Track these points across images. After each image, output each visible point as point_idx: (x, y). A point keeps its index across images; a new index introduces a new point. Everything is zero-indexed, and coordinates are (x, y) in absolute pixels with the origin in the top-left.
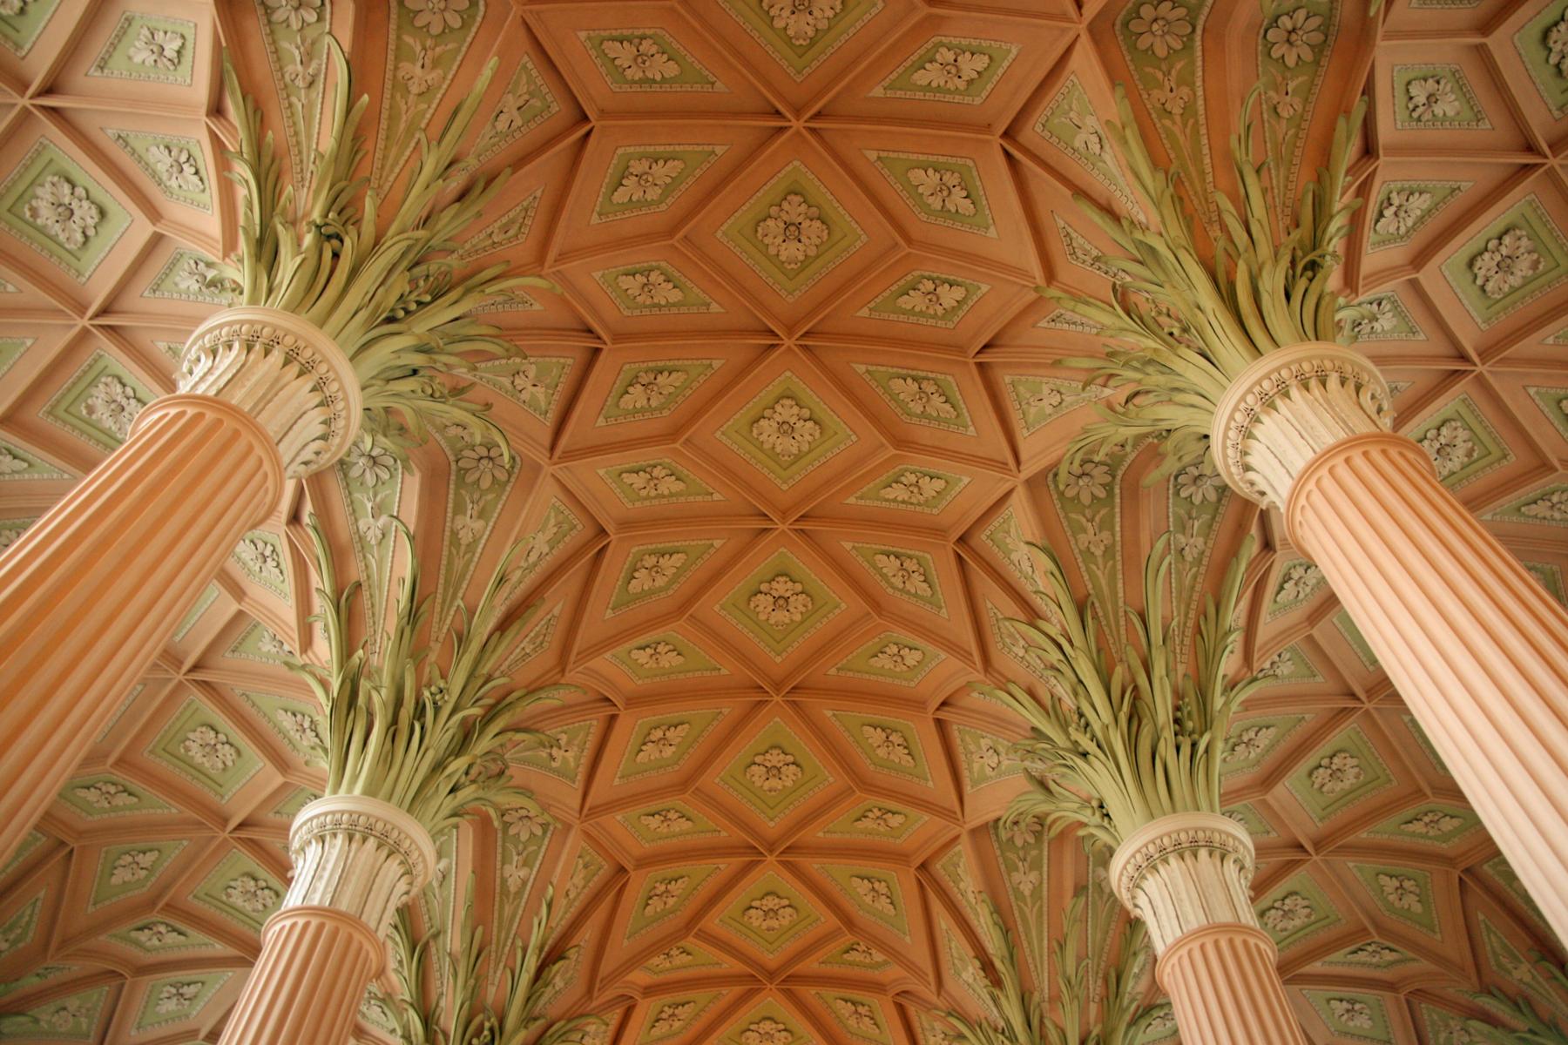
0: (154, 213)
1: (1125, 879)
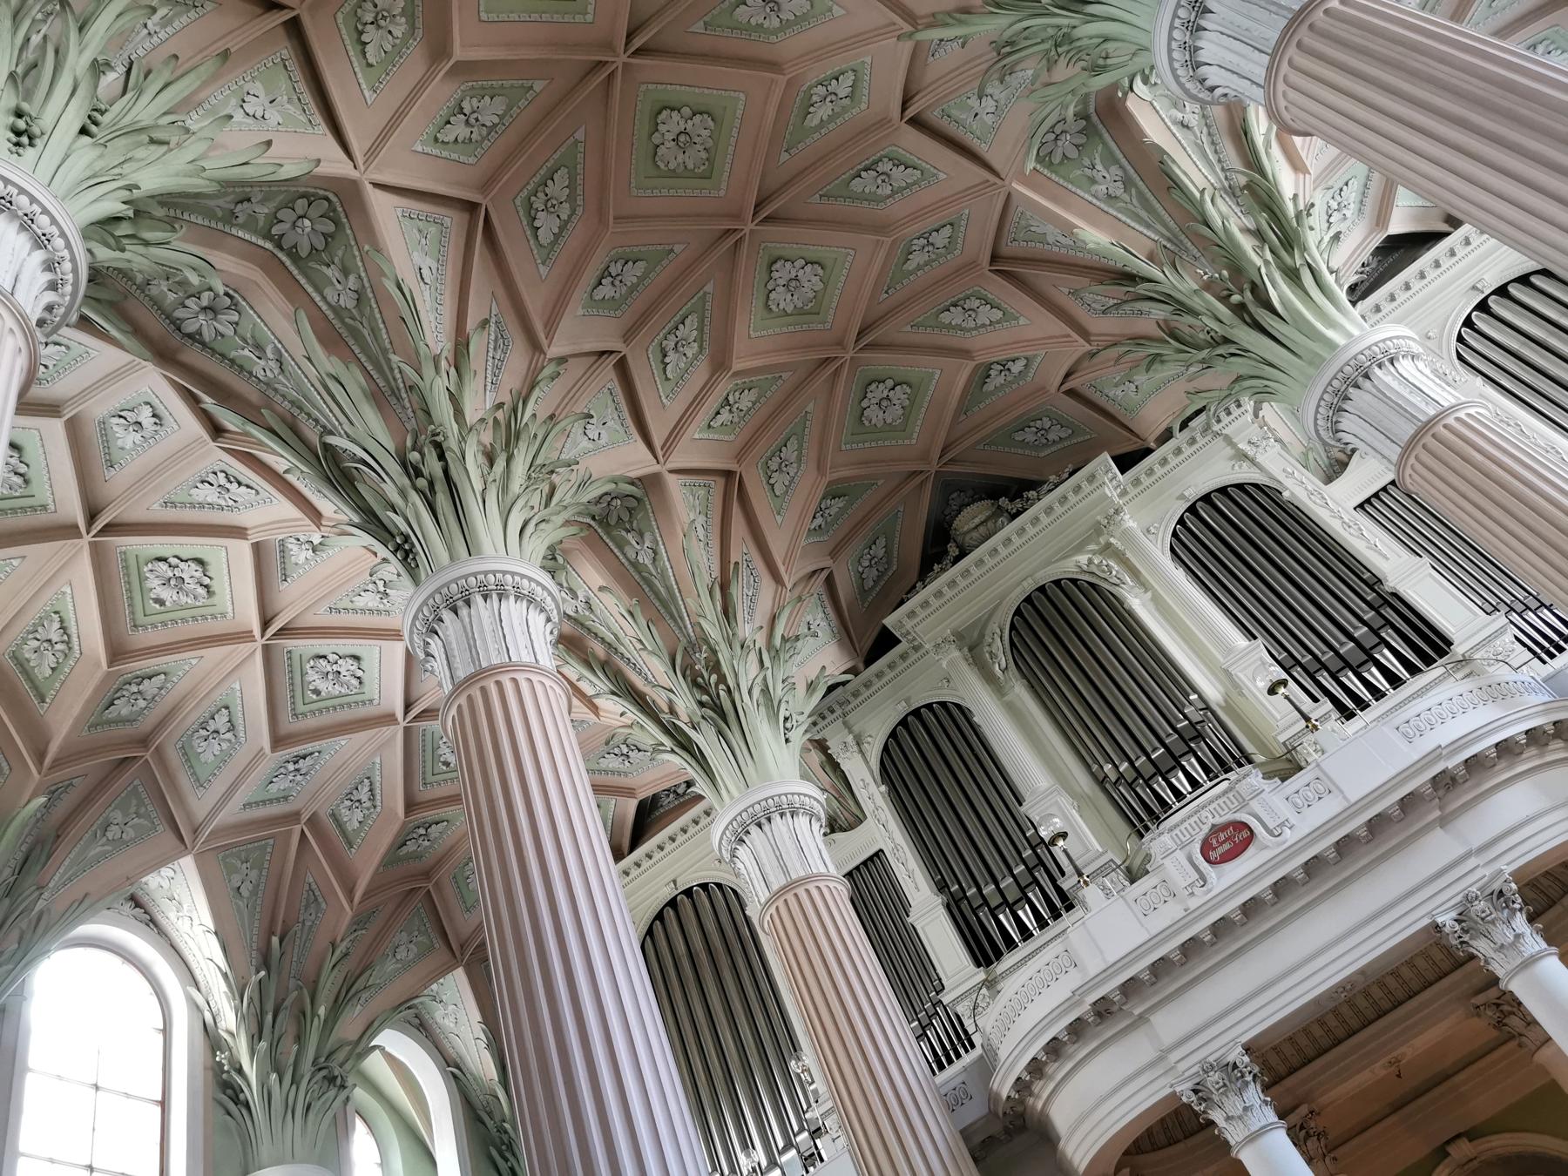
0: (238, 532)
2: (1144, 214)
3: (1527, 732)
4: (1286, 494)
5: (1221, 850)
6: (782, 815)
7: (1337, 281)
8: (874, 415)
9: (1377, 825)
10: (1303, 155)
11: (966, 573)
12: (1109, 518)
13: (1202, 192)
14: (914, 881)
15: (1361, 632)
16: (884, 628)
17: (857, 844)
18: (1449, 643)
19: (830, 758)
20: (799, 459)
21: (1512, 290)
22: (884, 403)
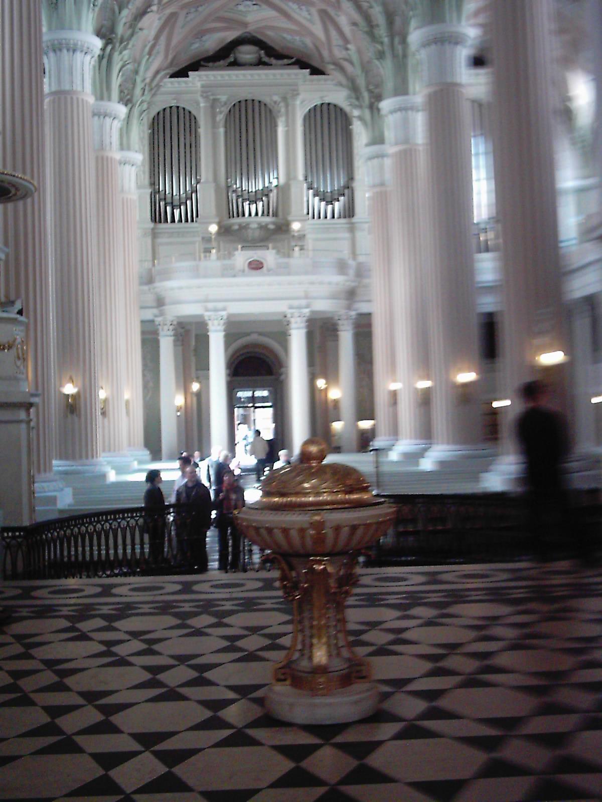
18: (353, 216)
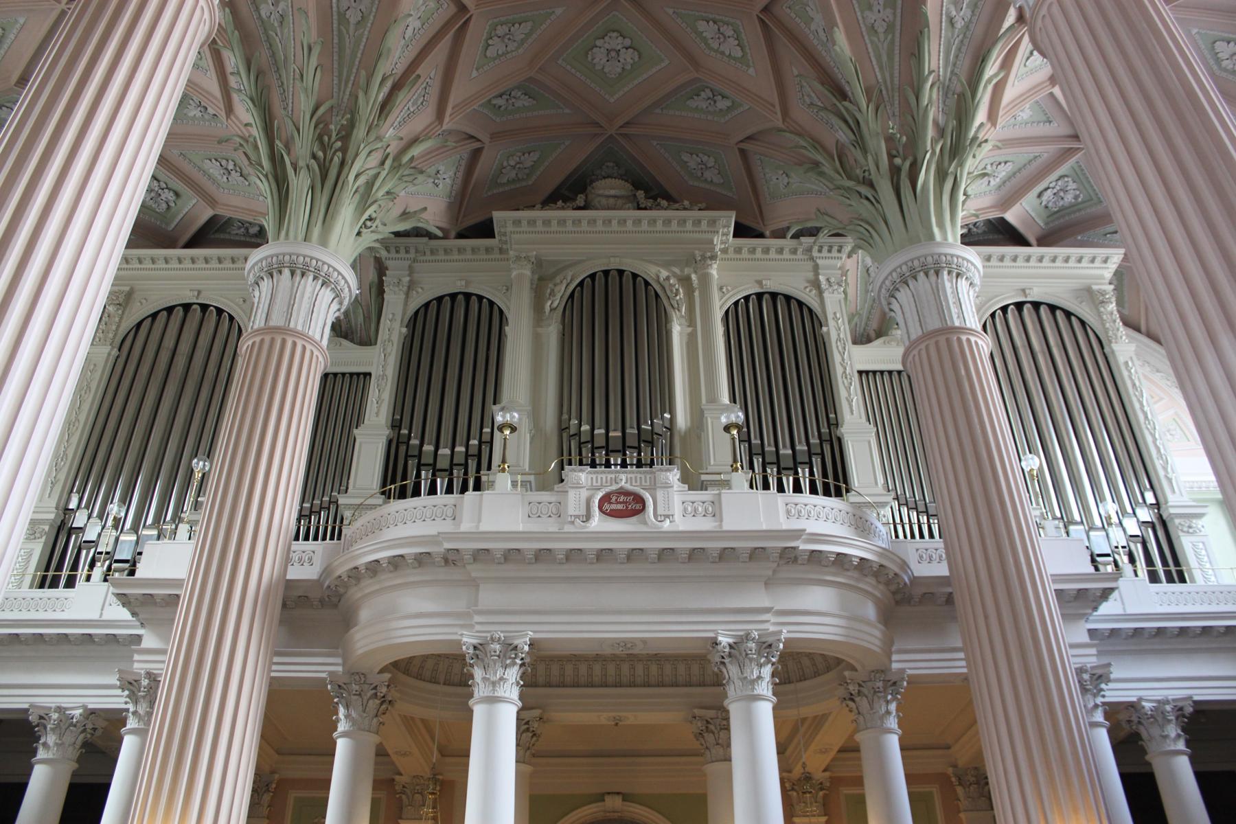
1: (883, 291)
2: (885, 58)
3: (862, 559)
4: (824, 329)
5: (614, 507)
6: (315, 278)
7: (964, 202)
8: (599, 57)
9: (725, 555)
10: (1001, 113)
11: (577, 222)
12: (704, 258)
13: (930, 72)
14: (378, 408)
15: (801, 447)
16: (491, 221)
17: (355, 358)
19: (381, 284)
20: (523, 41)
21: (1043, 309)
22: (613, 54)
